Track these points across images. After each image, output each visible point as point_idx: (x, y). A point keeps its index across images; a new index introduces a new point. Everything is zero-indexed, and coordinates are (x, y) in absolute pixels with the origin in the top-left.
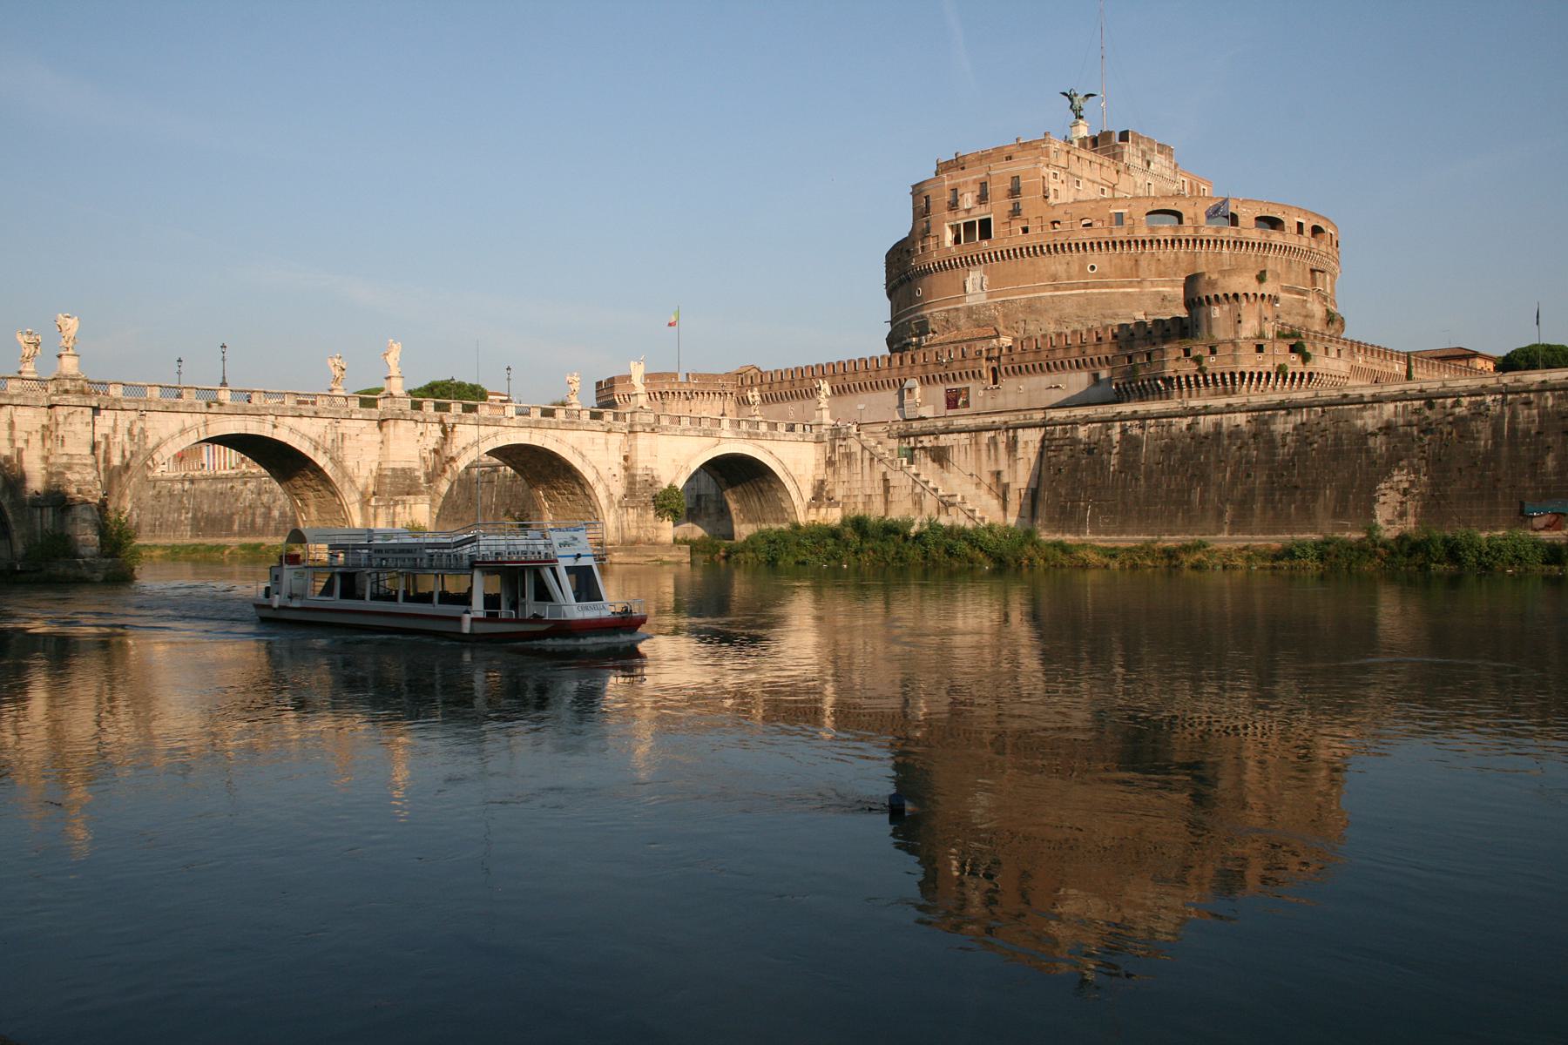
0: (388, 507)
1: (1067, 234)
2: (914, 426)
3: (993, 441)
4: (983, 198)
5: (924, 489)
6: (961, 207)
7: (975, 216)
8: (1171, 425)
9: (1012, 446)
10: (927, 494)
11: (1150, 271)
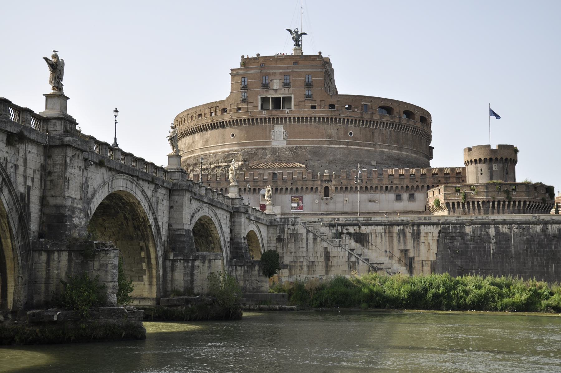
0: (186, 261)
1: (339, 113)
2: (341, 219)
3: (403, 232)
4: (286, 85)
5: (358, 259)
6: (271, 88)
7: (281, 94)
8: (529, 228)
9: (416, 236)
10: (361, 263)
11: (379, 139)
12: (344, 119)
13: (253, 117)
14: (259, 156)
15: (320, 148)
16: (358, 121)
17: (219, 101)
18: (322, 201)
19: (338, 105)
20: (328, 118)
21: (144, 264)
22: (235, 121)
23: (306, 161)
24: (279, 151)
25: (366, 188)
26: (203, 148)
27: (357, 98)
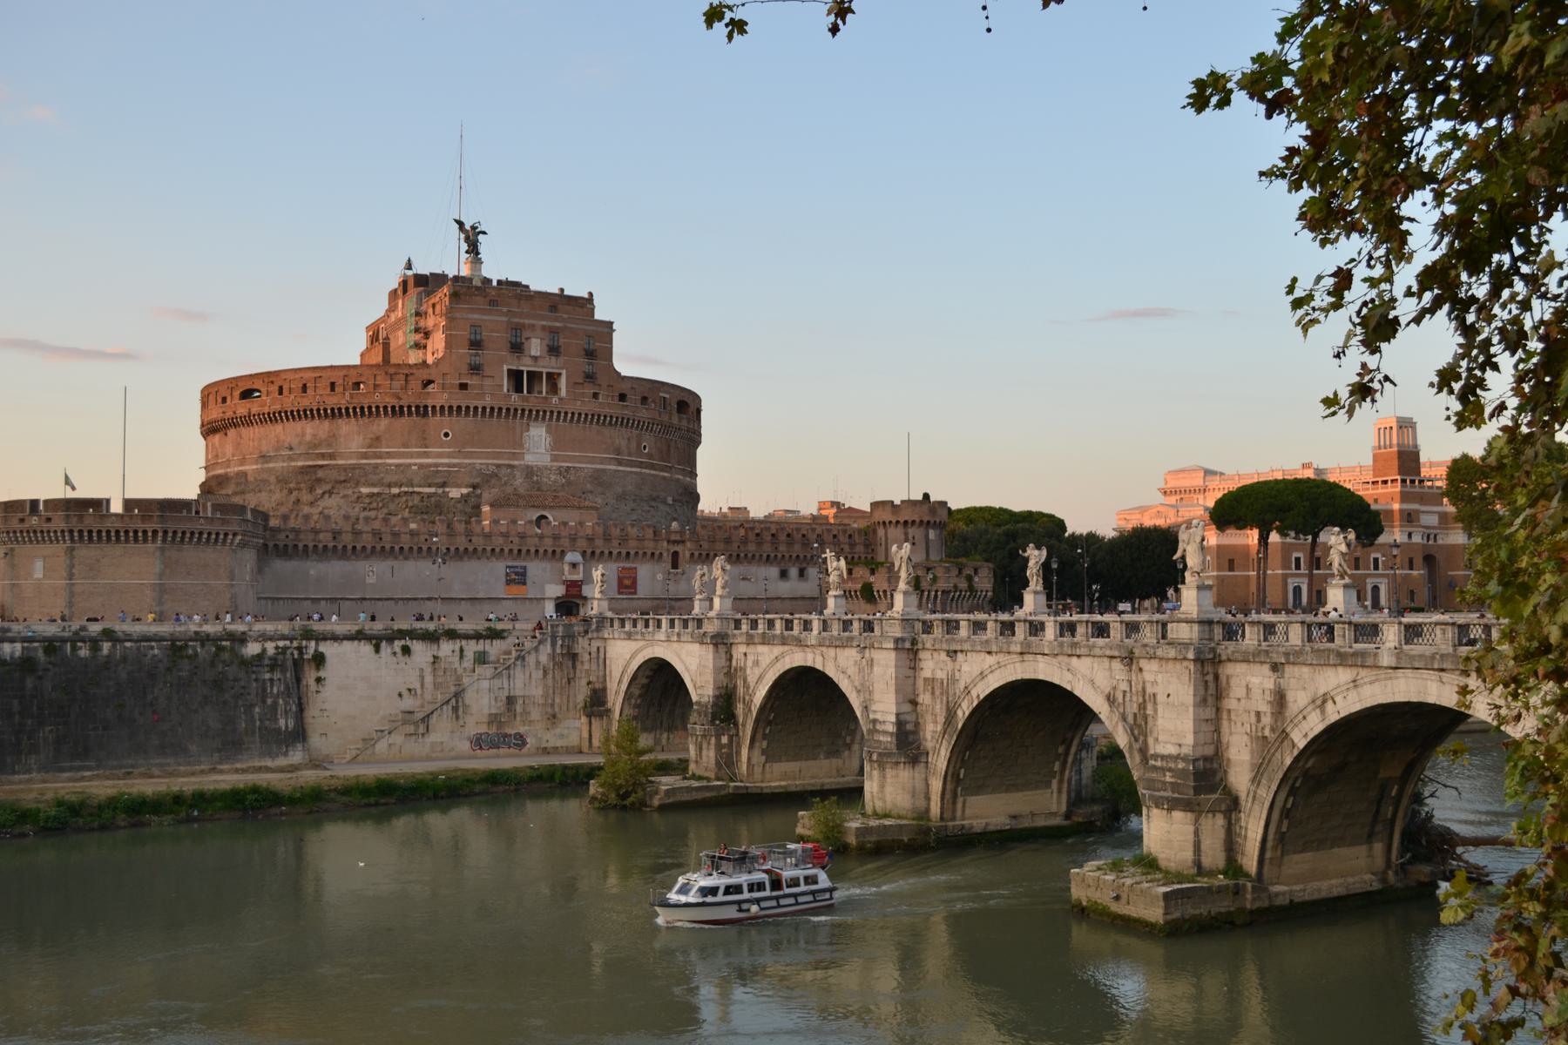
4: (553, 350)
7: (544, 367)
12: (639, 422)
14: (500, 479)
15: (604, 471)
21: (1057, 764)
25: (738, 555)
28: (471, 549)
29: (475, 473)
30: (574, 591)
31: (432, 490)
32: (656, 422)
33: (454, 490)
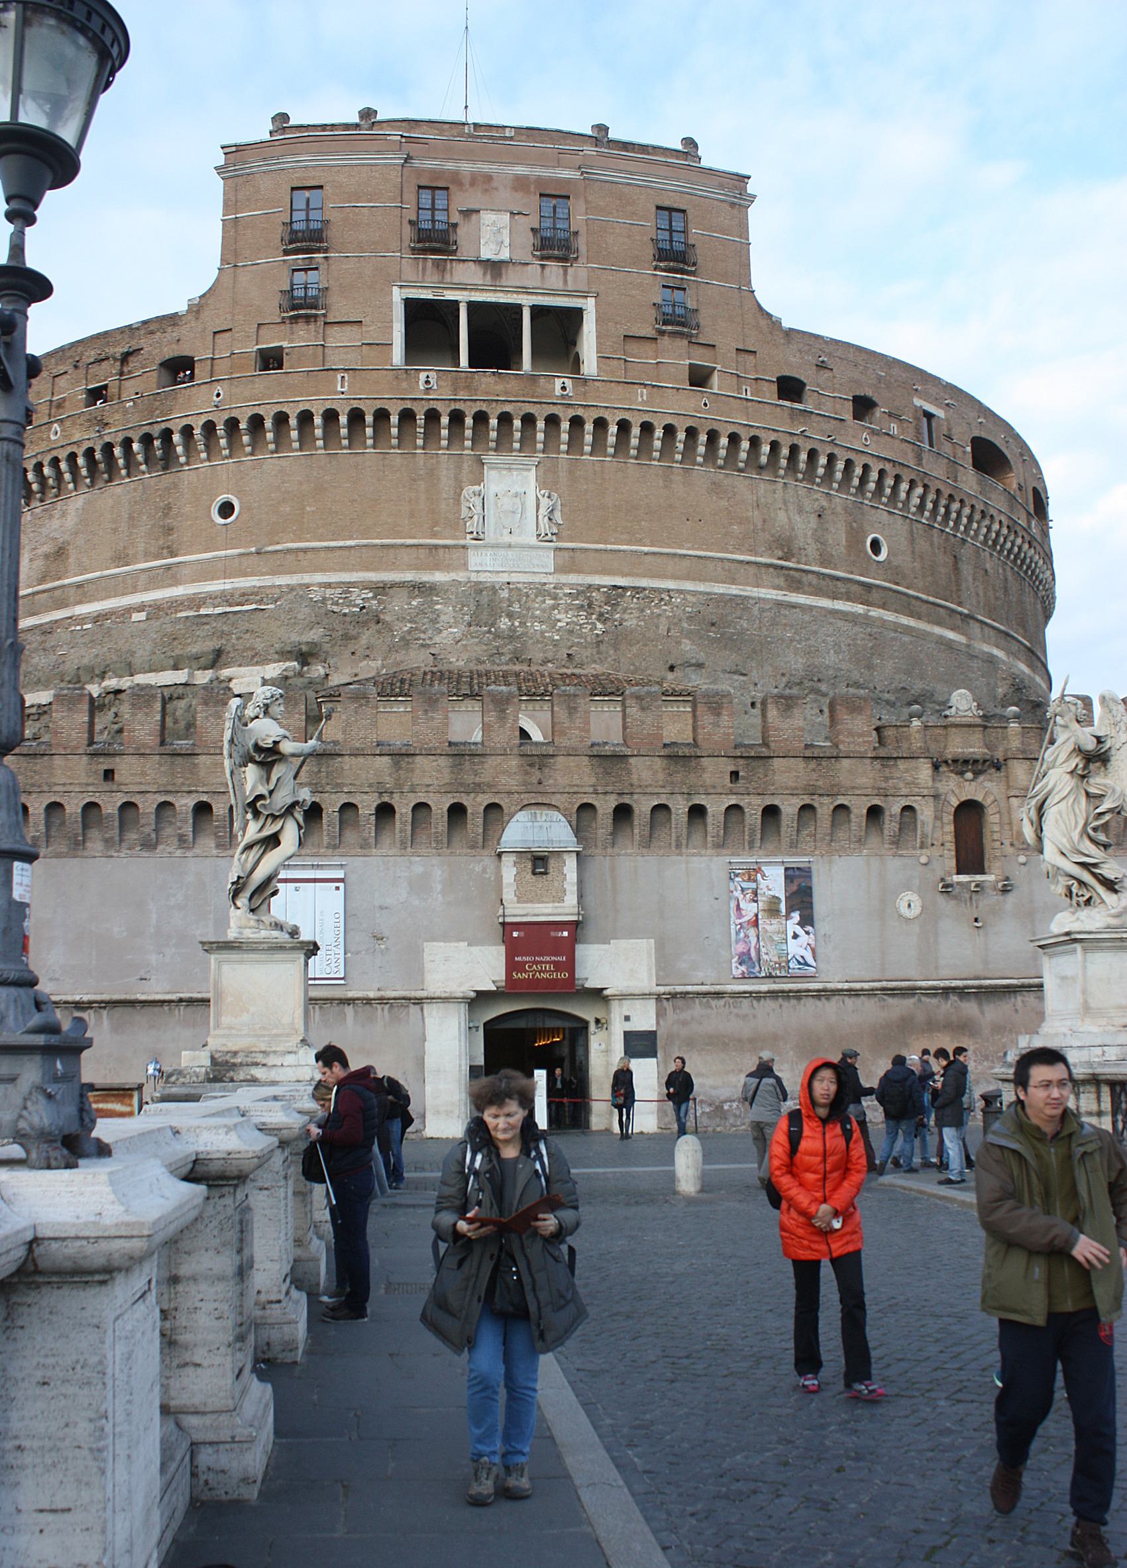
7: (526, 291)
11: (978, 595)
12: (849, 464)
13: (355, 404)
16: (904, 486)
17: (145, 323)
18: (941, 900)
19: (818, 386)
20: (775, 446)
22: (243, 426)
23: (672, 668)
24: (516, 607)
26: (34, 594)
27: (895, 371)
28: (110, 806)
29: (304, 612)
30: (542, 968)
31: (181, 676)
32: (907, 476)
33: (242, 669)
